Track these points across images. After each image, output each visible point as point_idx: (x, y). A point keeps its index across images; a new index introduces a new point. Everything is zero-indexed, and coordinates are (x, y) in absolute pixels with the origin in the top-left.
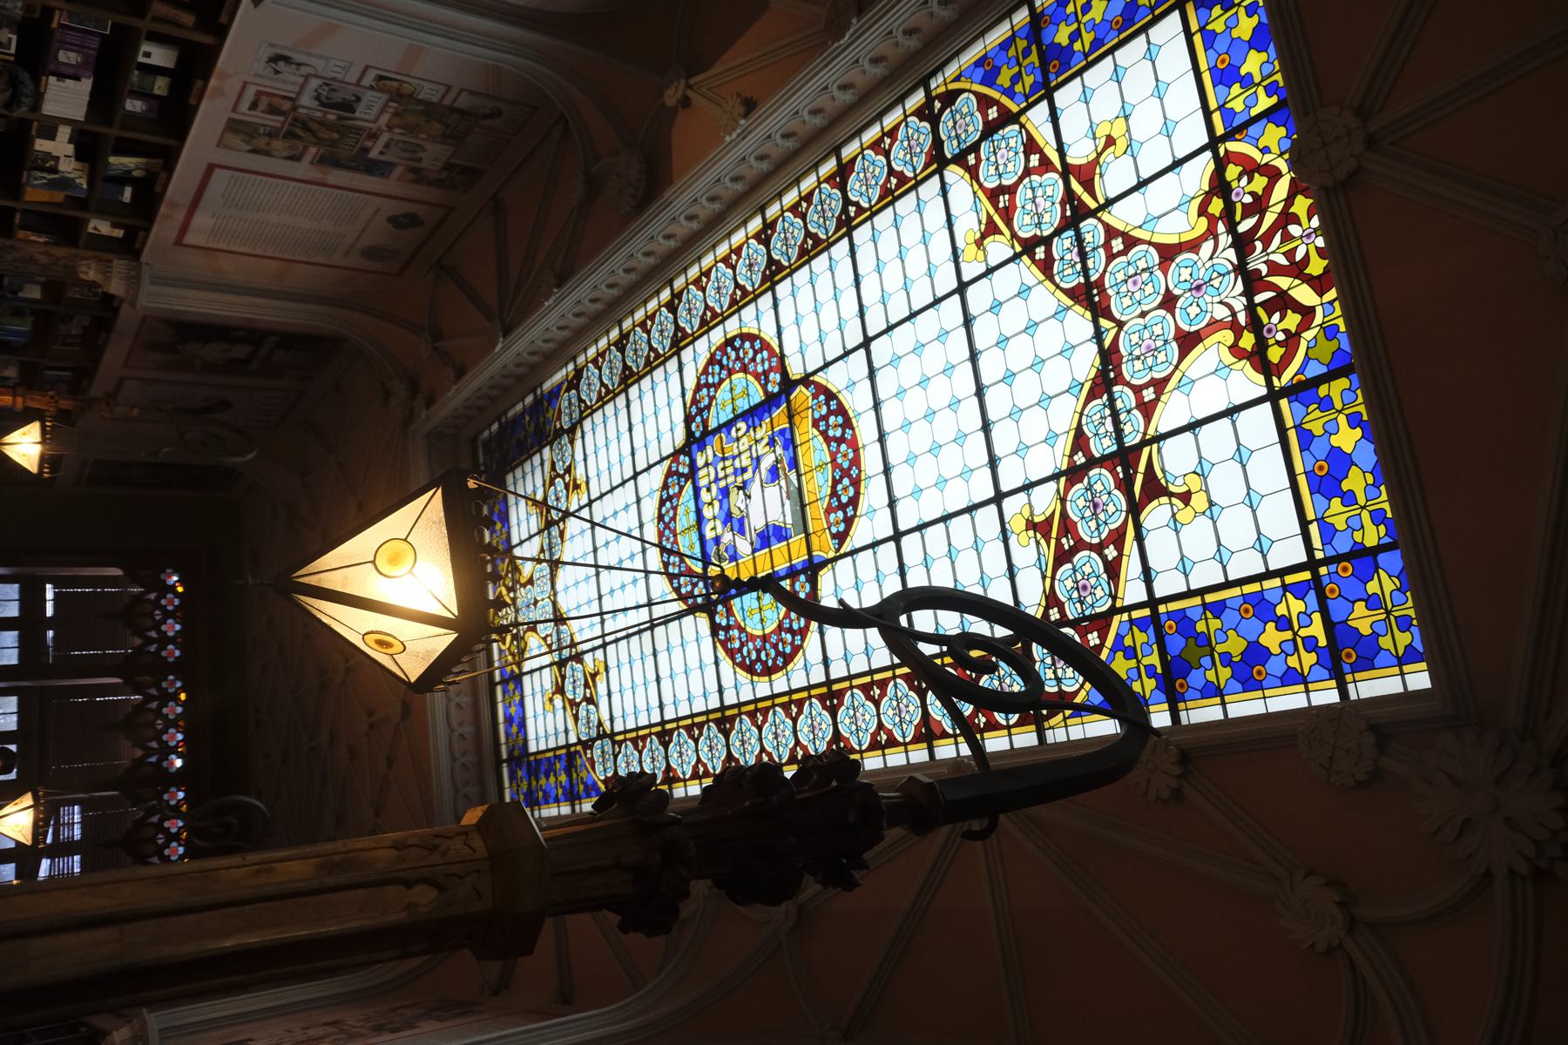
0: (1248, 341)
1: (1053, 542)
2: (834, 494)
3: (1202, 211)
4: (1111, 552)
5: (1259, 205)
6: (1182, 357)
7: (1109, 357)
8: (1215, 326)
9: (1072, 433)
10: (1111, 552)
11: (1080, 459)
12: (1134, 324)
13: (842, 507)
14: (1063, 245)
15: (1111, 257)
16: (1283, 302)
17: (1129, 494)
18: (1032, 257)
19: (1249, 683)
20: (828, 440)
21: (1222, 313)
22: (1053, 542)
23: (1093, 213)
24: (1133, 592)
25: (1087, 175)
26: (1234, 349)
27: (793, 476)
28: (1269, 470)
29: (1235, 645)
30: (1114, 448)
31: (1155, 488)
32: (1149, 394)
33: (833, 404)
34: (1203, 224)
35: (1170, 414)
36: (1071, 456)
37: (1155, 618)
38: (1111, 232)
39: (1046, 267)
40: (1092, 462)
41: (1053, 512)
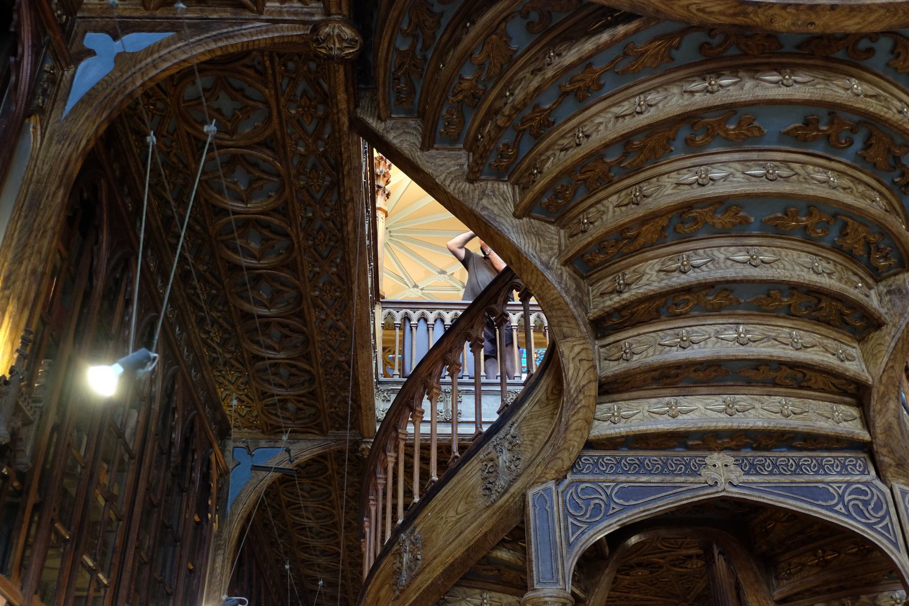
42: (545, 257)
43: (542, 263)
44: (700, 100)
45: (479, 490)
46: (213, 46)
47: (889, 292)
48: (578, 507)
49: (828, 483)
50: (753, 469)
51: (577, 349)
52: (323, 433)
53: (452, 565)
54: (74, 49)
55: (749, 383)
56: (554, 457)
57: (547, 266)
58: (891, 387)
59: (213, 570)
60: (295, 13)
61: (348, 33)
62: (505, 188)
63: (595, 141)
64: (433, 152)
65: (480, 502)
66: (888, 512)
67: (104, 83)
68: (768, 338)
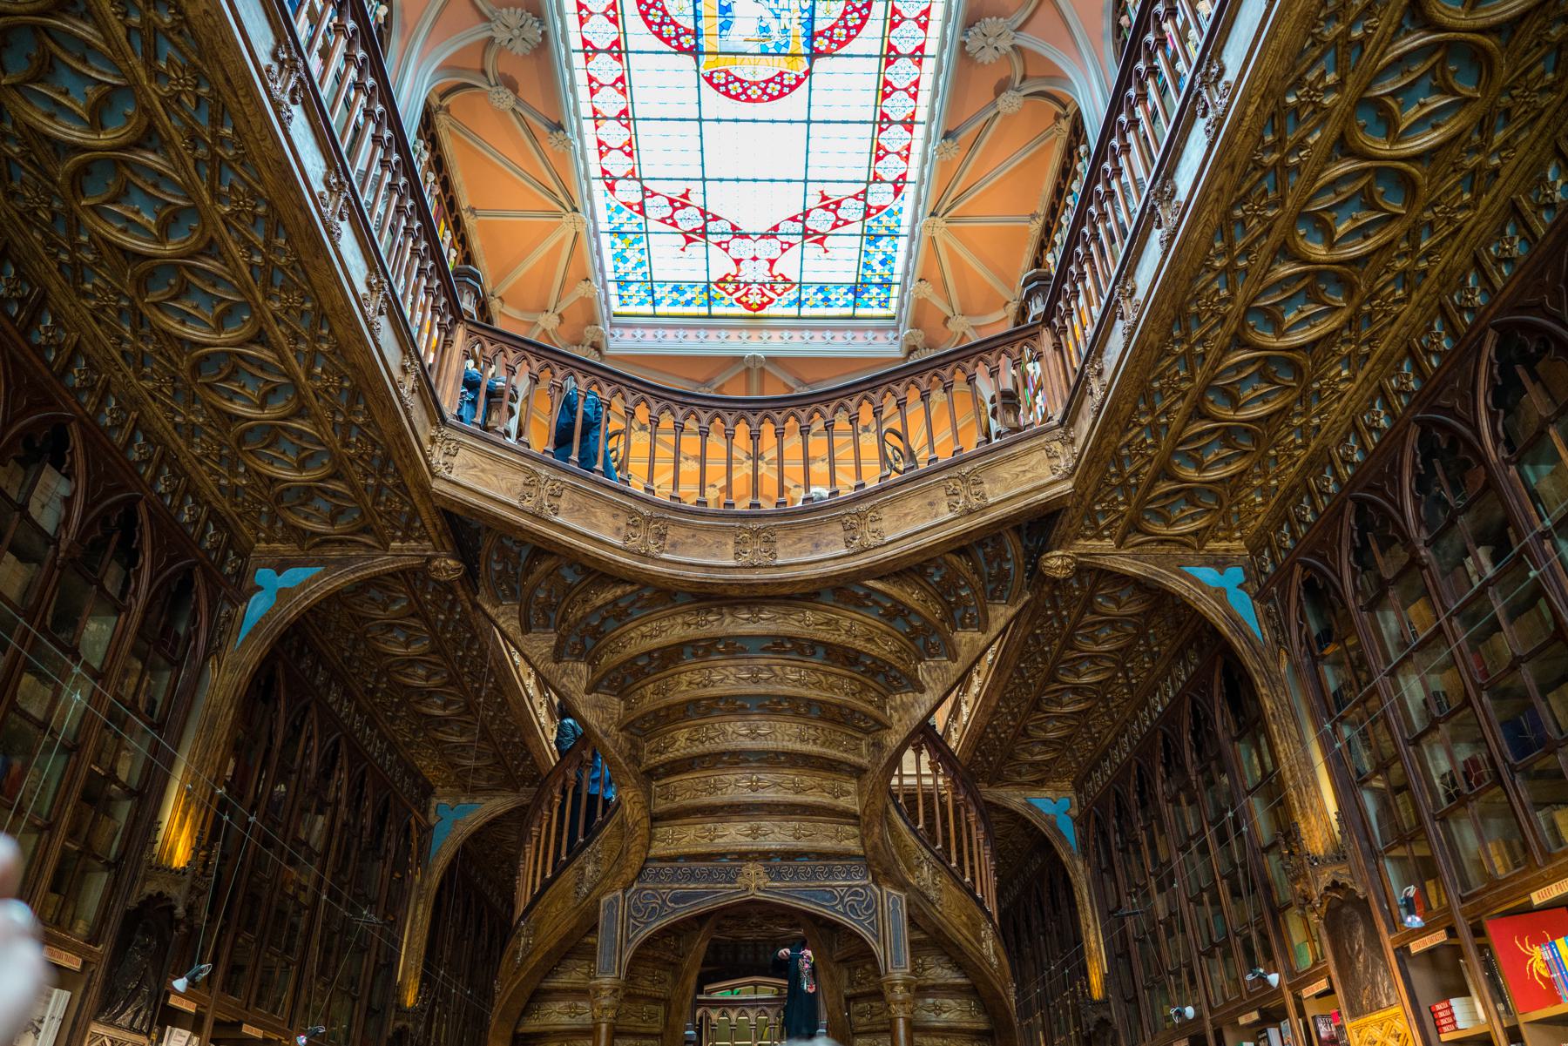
0: (730, 279)
2: (737, 79)
3: (782, 275)
4: (669, 221)
5: (772, 289)
7: (746, 236)
8: (739, 270)
10: (669, 221)
11: (709, 217)
12: (753, 245)
13: (726, 85)
14: (798, 227)
16: (737, 289)
19: (615, 257)
20: (767, 82)
24: (654, 226)
25: (820, 242)
27: (757, 49)
29: (628, 254)
31: (689, 240)
32: (724, 246)
33: (786, 90)
34: (775, 273)
38: (791, 245)
39: (794, 219)
40: (706, 221)
42: (605, 727)
43: (602, 731)
44: (692, 632)
45: (572, 894)
46: (352, 577)
47: (873, 744)
48: (639, 911)
49: (834, 887)
50: (779, 876)
51: (631, 795)
52: (516, 790)
53: (549, 952)
54: (247, 586)
55: (770, 813)
56: (619, 873)
57: (606, 734)
58: (874, 818)
59: (415, 917)
60: (413, 550)
62: (582, 667)
63: (632, 650)
64: (531, 635)
65: (571, 904)
66: (876, 910)
67: (267, 617)
68: (775, 784)
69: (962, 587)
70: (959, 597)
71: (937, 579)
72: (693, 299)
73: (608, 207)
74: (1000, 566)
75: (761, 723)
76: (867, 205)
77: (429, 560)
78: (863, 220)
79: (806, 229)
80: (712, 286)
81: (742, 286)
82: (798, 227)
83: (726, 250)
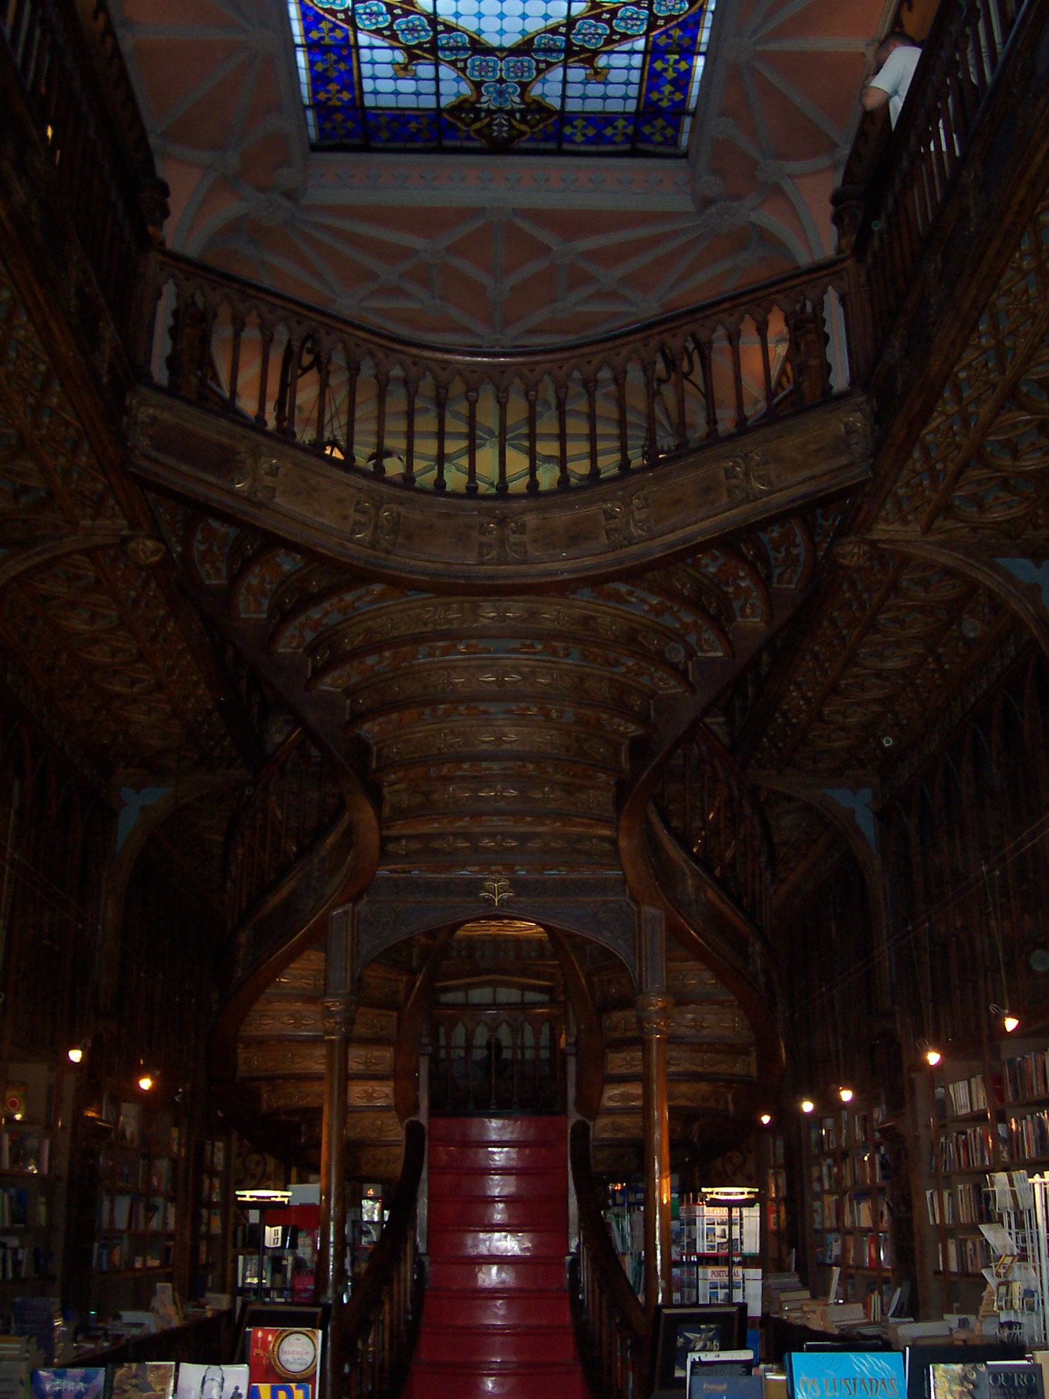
0: (467, 105)
1: (399, 4)
3: (535, 101)
5: (523, 121)
6: (472, 81)
7: (489, 51)
8: (480, 95)
9: (454, 26)
10: (386, 33)
11: (440, 28)
15: (538, 62)
16: (477, 118)
17: (415, 47)
18: (563, 25)
21: (484, 99)
22: (399, 4)
23: (565, 60)
24: (363, 39)
26: (466, 100)
28: (407, 102)
30: (439, 44)
32: (460, 65)
34: (528, 100)
35: (446, 72)
36: (444, 24)
37: (349, 47)
38: (550, 65)
39: (554, 31)
40: (436, 33)
41: (416, 8)
61: (150, 544)
69: (742, 578)
70: (738, 588)
71: (712, 570)
72: (419, 130)
73: (304, 16)
74: (787, 549)
75: (507, 730)
76: (651, 13)
77: (125, 540)
78: (646, 34)
79: (569, 43)
80: (446, 116)
81: (483, 115)
82: (560, 41)
83: (463, 70)
